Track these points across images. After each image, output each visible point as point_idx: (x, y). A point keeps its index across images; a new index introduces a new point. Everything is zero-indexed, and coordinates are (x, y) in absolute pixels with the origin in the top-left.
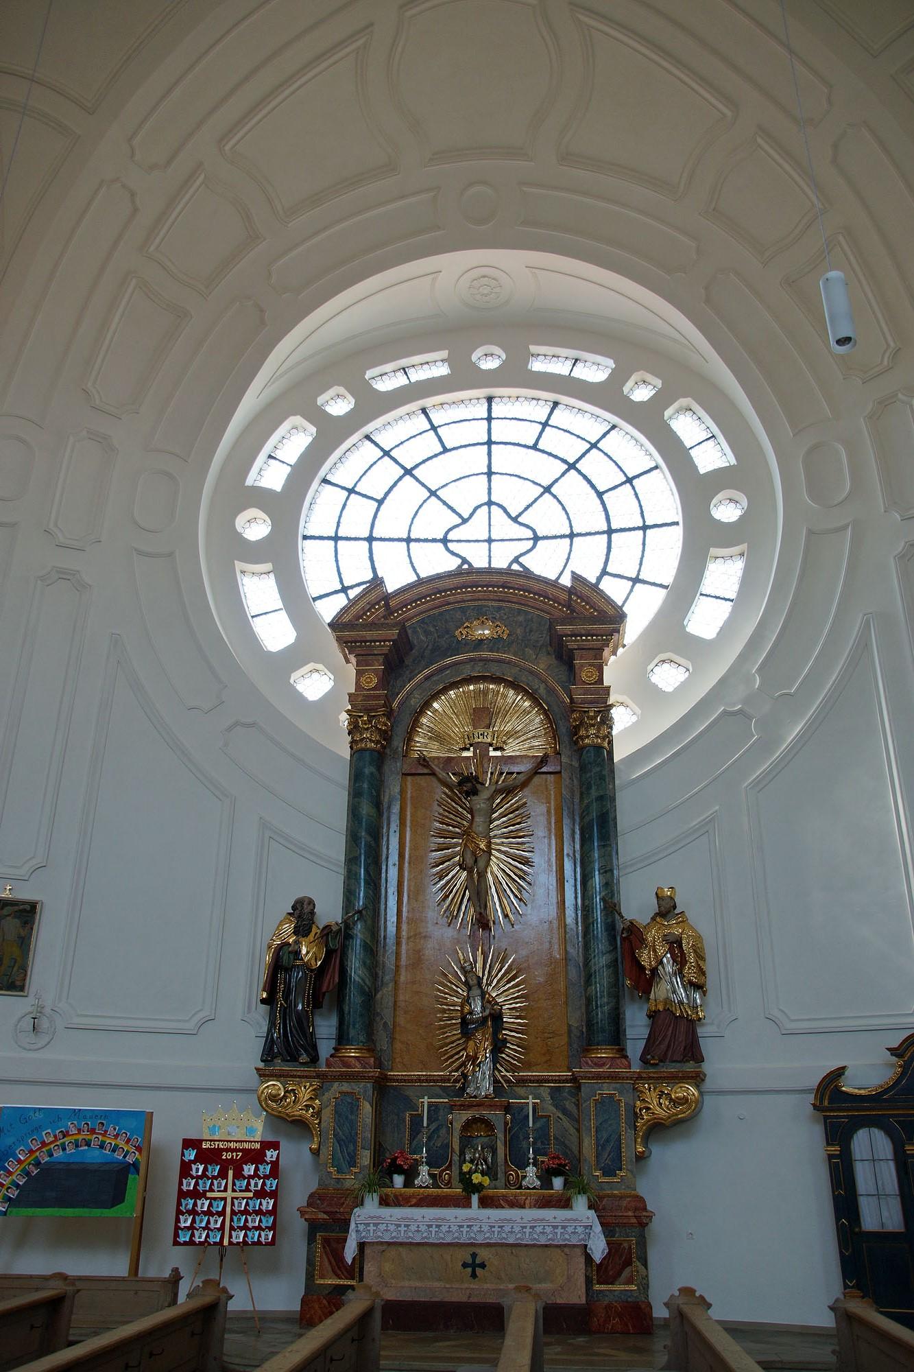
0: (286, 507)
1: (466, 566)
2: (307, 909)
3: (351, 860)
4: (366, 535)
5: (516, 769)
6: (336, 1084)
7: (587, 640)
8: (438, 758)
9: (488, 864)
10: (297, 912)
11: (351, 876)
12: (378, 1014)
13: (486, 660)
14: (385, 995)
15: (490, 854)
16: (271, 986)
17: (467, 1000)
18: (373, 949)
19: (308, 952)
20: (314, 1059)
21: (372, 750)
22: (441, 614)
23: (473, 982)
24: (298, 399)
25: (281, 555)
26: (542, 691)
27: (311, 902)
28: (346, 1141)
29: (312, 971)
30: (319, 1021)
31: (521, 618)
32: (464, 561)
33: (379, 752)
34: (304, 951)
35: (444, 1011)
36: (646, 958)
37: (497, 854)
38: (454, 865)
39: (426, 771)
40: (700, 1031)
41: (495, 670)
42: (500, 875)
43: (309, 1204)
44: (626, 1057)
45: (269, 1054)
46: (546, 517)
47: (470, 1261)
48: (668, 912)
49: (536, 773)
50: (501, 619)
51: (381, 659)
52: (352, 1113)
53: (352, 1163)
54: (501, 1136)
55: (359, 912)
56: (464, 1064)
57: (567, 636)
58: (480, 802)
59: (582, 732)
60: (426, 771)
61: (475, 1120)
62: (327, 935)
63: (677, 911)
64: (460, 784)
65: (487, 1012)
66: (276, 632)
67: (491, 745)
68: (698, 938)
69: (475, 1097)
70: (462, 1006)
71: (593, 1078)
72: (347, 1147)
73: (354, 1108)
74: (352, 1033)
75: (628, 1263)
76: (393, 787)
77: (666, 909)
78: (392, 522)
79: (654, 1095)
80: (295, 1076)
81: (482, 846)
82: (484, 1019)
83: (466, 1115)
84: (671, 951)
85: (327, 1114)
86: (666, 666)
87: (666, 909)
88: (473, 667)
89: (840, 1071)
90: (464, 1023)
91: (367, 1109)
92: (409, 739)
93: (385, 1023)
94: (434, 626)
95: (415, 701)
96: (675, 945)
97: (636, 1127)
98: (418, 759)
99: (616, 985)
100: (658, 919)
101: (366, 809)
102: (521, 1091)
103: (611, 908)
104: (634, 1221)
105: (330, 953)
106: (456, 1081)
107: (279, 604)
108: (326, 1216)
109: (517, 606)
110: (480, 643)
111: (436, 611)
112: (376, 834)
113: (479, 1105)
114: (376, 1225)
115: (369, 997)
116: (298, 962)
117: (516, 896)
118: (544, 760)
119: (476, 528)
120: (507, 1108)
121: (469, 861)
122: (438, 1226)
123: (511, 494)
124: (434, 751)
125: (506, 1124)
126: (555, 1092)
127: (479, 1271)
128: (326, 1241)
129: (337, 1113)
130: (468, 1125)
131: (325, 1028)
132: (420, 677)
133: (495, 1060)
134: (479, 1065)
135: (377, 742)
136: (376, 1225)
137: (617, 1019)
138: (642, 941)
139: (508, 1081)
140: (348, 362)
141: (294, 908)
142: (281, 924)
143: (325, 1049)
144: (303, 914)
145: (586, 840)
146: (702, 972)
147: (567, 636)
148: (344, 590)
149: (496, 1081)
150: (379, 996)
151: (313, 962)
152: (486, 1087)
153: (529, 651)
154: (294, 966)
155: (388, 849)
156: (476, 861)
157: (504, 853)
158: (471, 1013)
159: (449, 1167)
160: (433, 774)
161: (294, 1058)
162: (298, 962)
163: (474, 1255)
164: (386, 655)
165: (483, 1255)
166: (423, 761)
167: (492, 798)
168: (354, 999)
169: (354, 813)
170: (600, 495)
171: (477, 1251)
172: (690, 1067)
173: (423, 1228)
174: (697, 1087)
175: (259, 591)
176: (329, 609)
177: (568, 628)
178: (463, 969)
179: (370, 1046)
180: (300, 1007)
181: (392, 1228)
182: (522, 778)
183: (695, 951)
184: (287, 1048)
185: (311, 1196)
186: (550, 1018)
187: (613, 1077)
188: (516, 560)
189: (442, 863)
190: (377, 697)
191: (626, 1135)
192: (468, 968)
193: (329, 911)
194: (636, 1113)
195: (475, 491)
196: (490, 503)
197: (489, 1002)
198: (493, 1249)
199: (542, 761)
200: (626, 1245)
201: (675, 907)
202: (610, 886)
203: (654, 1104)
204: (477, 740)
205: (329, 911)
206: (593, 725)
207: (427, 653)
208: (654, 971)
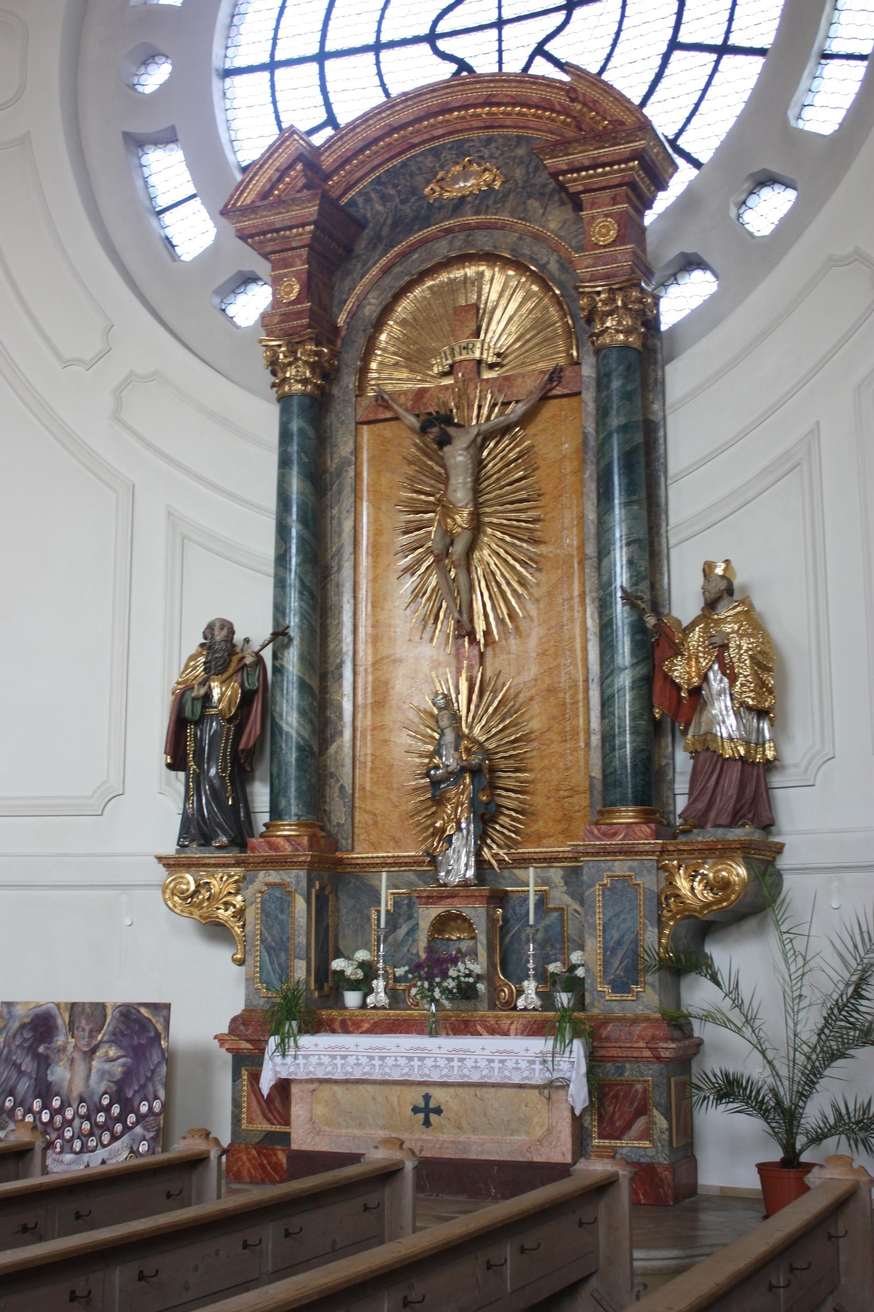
4: (315, 50)
7: (597, 175)
12: (332, 775)
13: (468, 228)
22: (404, 165)
26: (553, 266)
28: (277, 947)
31: (521, 152)
32: (463, 65)
33: (310, 396)
39: (389, 415)
41: (483, 241)
42: (493, 561)
47: (422, 1104)
50: (492, 157)
51: (304, 252)
52: (282, 912)
57: (564, 173)
72: (278, 957)
73: (285, 904)
75: (643, 1110)
83: (434, 911)
84: (720, 659)
85: (251, 914)
86: (766, 192)
87: (720, 593)
88: (451, 242)
93: (342, 787)
94: (395, 186)
95: (371, 310)
104: (647, 1053)
108: (249, 1046)
109: (513, 132)
111: (396, 162)
113: (452, 896)
114: (421, 1059)
116: (213, 711)
122: (461, 1060)
127: (433, 1117)
129: (265, 913)
132: (375, 271)
136: (421, 1059)
139: (500, 861)
147: (564, 173)
153: (533, 204)
163: (427, 1098)
164: (310, 246)
165: (439, 1096)
166: (382, 401)
171: (433, 1091)
173: (482, 1064)
175: (167, 171)
177: (561, 162)
180: (213, 772)
181: (402, 1062)
185: (234, 1020)
186: (567, 769)
188: (540, 51)
190: (298, 315)
198: (452, 1090)
199: (551, 380)
200: (639, 1087)
206: (610, 313)
207: (384, 233)
208: (696, 692)
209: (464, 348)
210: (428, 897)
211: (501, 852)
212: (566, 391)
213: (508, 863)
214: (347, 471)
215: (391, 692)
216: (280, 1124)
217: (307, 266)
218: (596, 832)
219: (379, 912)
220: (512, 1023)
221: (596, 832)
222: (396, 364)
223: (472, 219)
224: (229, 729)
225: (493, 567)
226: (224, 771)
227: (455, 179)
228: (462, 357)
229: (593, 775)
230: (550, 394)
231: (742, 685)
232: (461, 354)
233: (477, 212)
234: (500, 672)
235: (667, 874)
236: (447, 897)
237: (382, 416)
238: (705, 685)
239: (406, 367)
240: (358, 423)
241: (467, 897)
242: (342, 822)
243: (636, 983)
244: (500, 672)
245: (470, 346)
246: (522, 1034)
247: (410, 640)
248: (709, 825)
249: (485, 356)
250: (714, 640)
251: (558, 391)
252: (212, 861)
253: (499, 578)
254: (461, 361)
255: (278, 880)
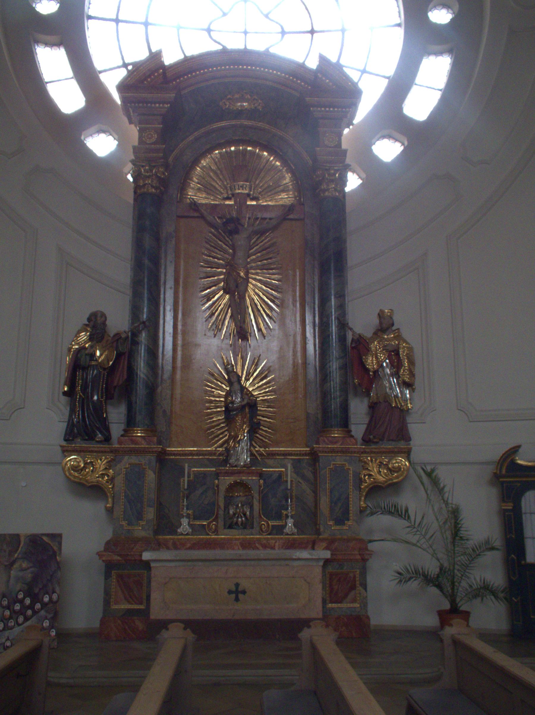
2: (100, 320)
3: (136, 284)
5: (267, 215)
6: (126, 457)
8: (206, 204)
9: (246, 290)
10: (92, 323)
11: (136, 295)
14: (163, 390)
15: (248, 282)
16: (72, 382)
17: (229, 394)
18: (153, 352)
19: (101, 355)
20: (107, 439)
21: (151, 194)
23: (234, 379)
27: (103, 315)
29: (105, 369)
30: (110, 409)
34: (98, 353)
35: (211, 402)
36: (371, 362)
37: (254, 282)
38: (219, 290)
39: (196, 214)
40: (409, 419)
42: (256, 298)
43: (106, 550)
44: (352, 436)
45: (70, 435)
47: (234, 589)
48: (387, 329)
49: (285, 219)
53: (140, 516)
54: (256, 496)
55: (144, 323)
56: (227, 442)
58: (241, 239)
59: (324, 186)
60: (196, 214)
61: (236, 483)
62: (117, 340)
63: (394, 328)
64: (225, 224)
65: (245, 402)
66: (67, 97)
67: (248, 195)
68: (410, 349)
69: (236, 466)
70: (226, 397)
71: (328, 452)
74: (139, 418)
76: (168, 227)
77: (385, 325)
79: (375, 465)
80: (92, 451)
81: (242, 274)
82: (243, 407)
83: (230, 480)
85: (119, 481)
87: (385, 325)
89: (515, 450)
90: (228, 410)
91: (151, 476)
92: (183, 188)
93: (164, 411)
96: (394, 355)
97: (360, 488)
98: (191, 203)
99: (344, 384)
100: (379, 333)
101: (148, 242)
102: (270, 462)
103: (343, 325)
104: (358, 557)
105: (119, 356)
106: (220, 455)
107: (71, 74)
108: (119, 558)
110: (239, 114)
112: (156, 261)
113: (239, 472)
115: (152, 389)
116: (93, 363)
117: (268, 315)
118: (290, 209)
120: (261, 475)
121: (232, 285)
124: (202, 199)
125: (260, 486)
126: (297, 464)
127: (241, 596)
128: (120, 577)
130: (232, 487)
131: (116, 415)
132: (191, 138)
133: (251, 438)
134: (239, 442)
135: (156, 188)
137: (345, 408)
138: (368, 350)
139: (261, 455)
141: (89, 320)
142: (79, 332)
143: (116, 430)
144: (96, 325)
145: (324, 272)
146: (412, 374)
148: (125, 65)
149: (252, 455)
150: (159, 389)
151: (106, 362)
152: (245, 458)
154: (89, 366)
155: (165, 276)
156: (237, 287)
157: (260, 281)
158: (233, 402)
159: (216, 519)
160: (202, 217)
161: (91, 437)
162: (93, 363)
166: (195, 206)
167: (249, 238)
168: (141, 390)
169: (138, 244)
172: (402, 445)
174: (408, 459)
175: (52, 63)
178: (226, 370)
179: (151, 429)
180: (96, 398)
182: (274, 222)
183: (408, 358)
184: (85, 429)
185: (108, 543)
187: (344, 452)
189: (210, 288)
191: (353, 495)
192: (231, 369)
193: (118, 321)
194: (360, 479)
197: (247, 395)
199: (289, 210)
200: (351, 575)
201: (393, 325)
202: (341, 307)
203: (374, 471)
204: (237, 191)
205: (118, 321)
209: (241, 187)
210: (226, 473)
211: (261, 449)
212: (296, 217)
213: (265, 456)
214: (171, 241)
215: (193, 361)
216: (137, 604)
217: (161, 126)
218: (326, 441)
219: (184, 480)
220: (276, 542)
221: (326, 441)
222: (199, 189)
223: (246, 123)
224: (104, 375)
225: (256, 301)
226: (102, 398)
227: (238, 100)
228: (240, 191)
229: (309, 411)
230: (287, 217)
231: (404, 371)
232: (239, 189)
233: (249, 119)
234: (260, 355)
235: (363, 464)
236: (237, 473)
237: (192, 215)
238: (380, 370)
239: (205, 192)
240: (179, 217)
241: (249, 473)
242: (164, 430)
243: (348, 520)
244: (260, 355)
245: (245, 186)
246: (282, 547)
247: (205, 335)
248: (385, 439)
249: (252, 193)
250: (388, 348)
251: (291, 216)
252: (96, 449)
253: (259, 307)
254: (239, 193)
255: (137, 462)
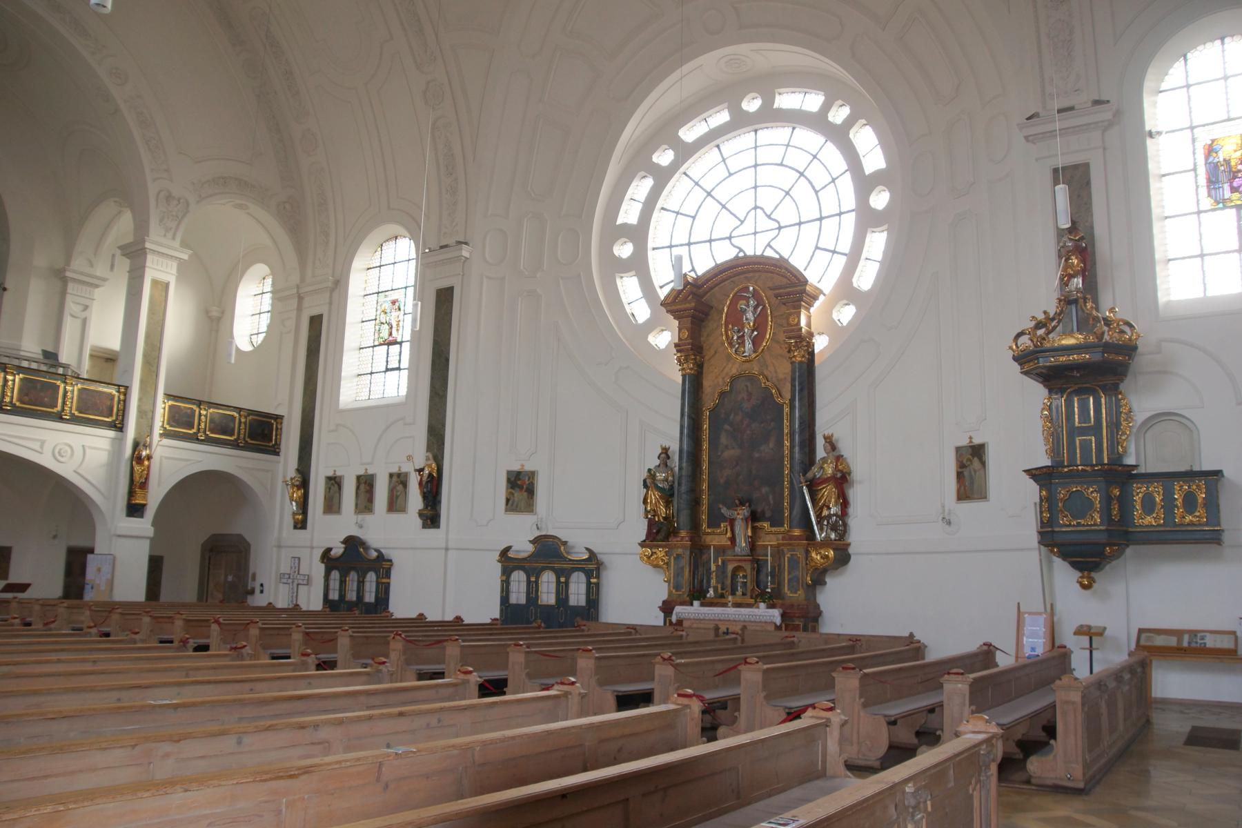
0: (638, 233)
1: (741, 254)
24: (639, 163)
25: (639, 265)
32: (741, 250)
46: (786, 214)
78: (700, 233)
119: (748, 227)
123: (768, 199)
140: (665, 132)
170: (816, 192)
175: (629, 287)
176: (663, 294)
188: (769, 245)
195: (746, 201)
196: (756, 208)
